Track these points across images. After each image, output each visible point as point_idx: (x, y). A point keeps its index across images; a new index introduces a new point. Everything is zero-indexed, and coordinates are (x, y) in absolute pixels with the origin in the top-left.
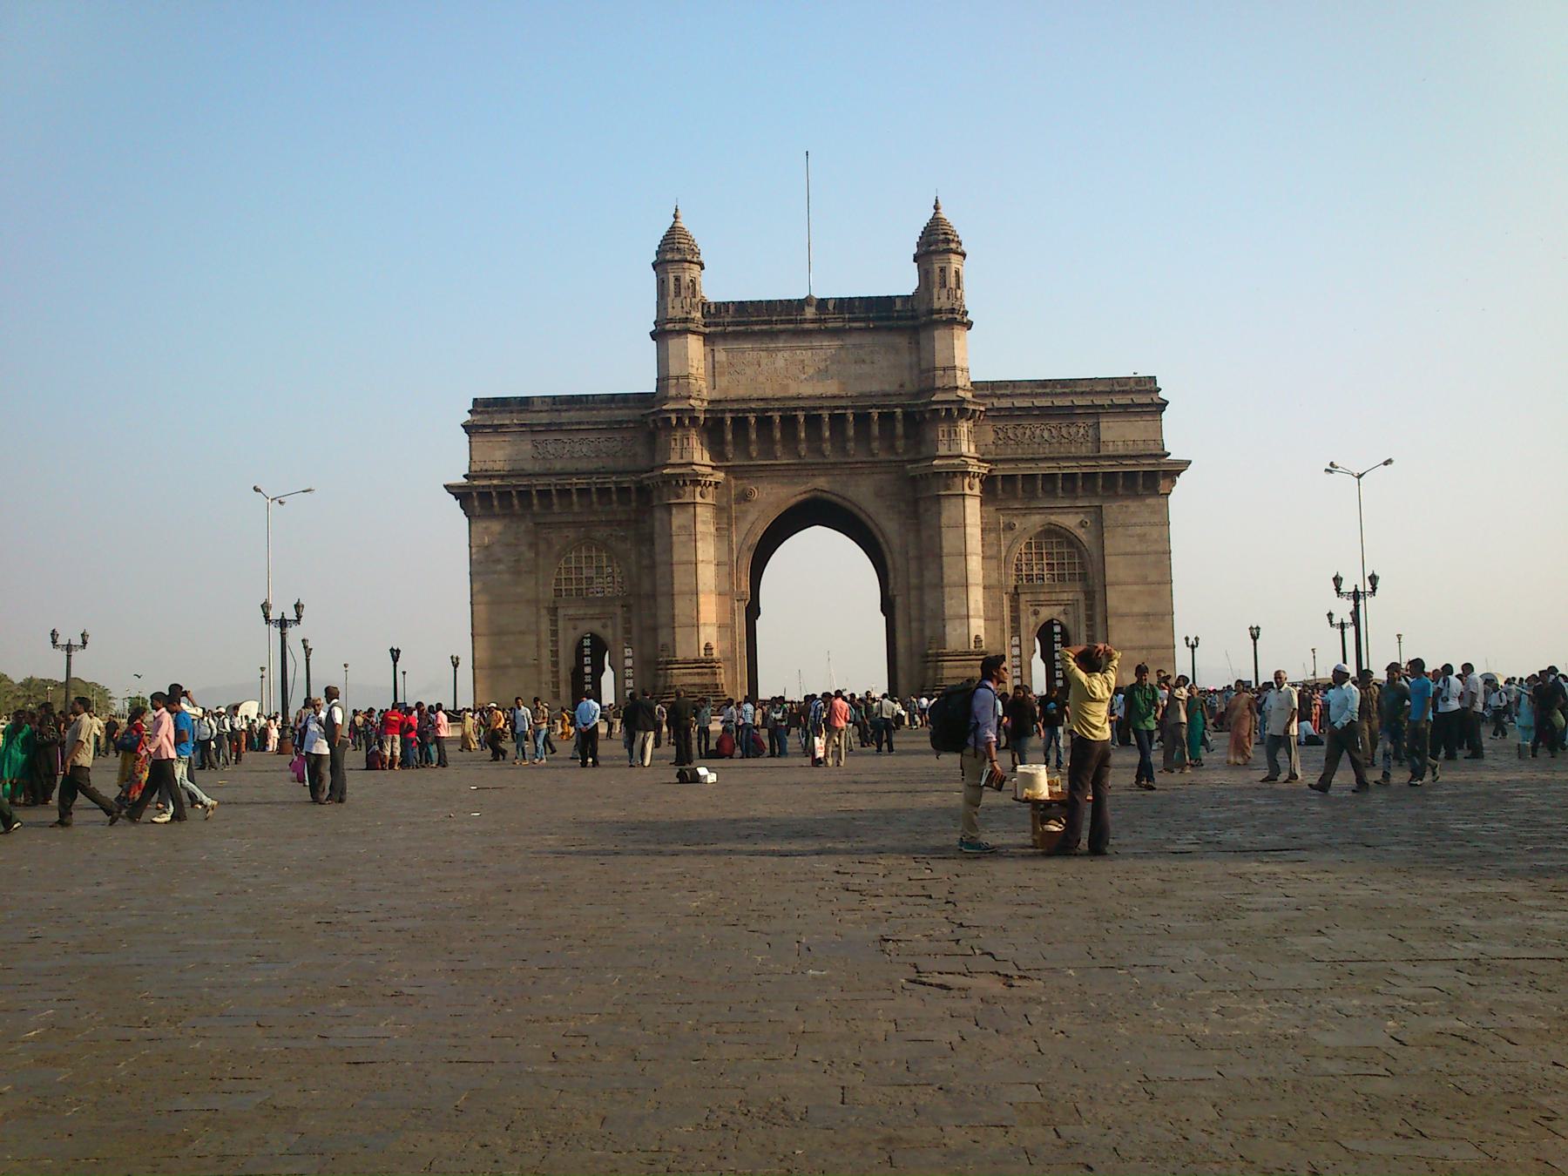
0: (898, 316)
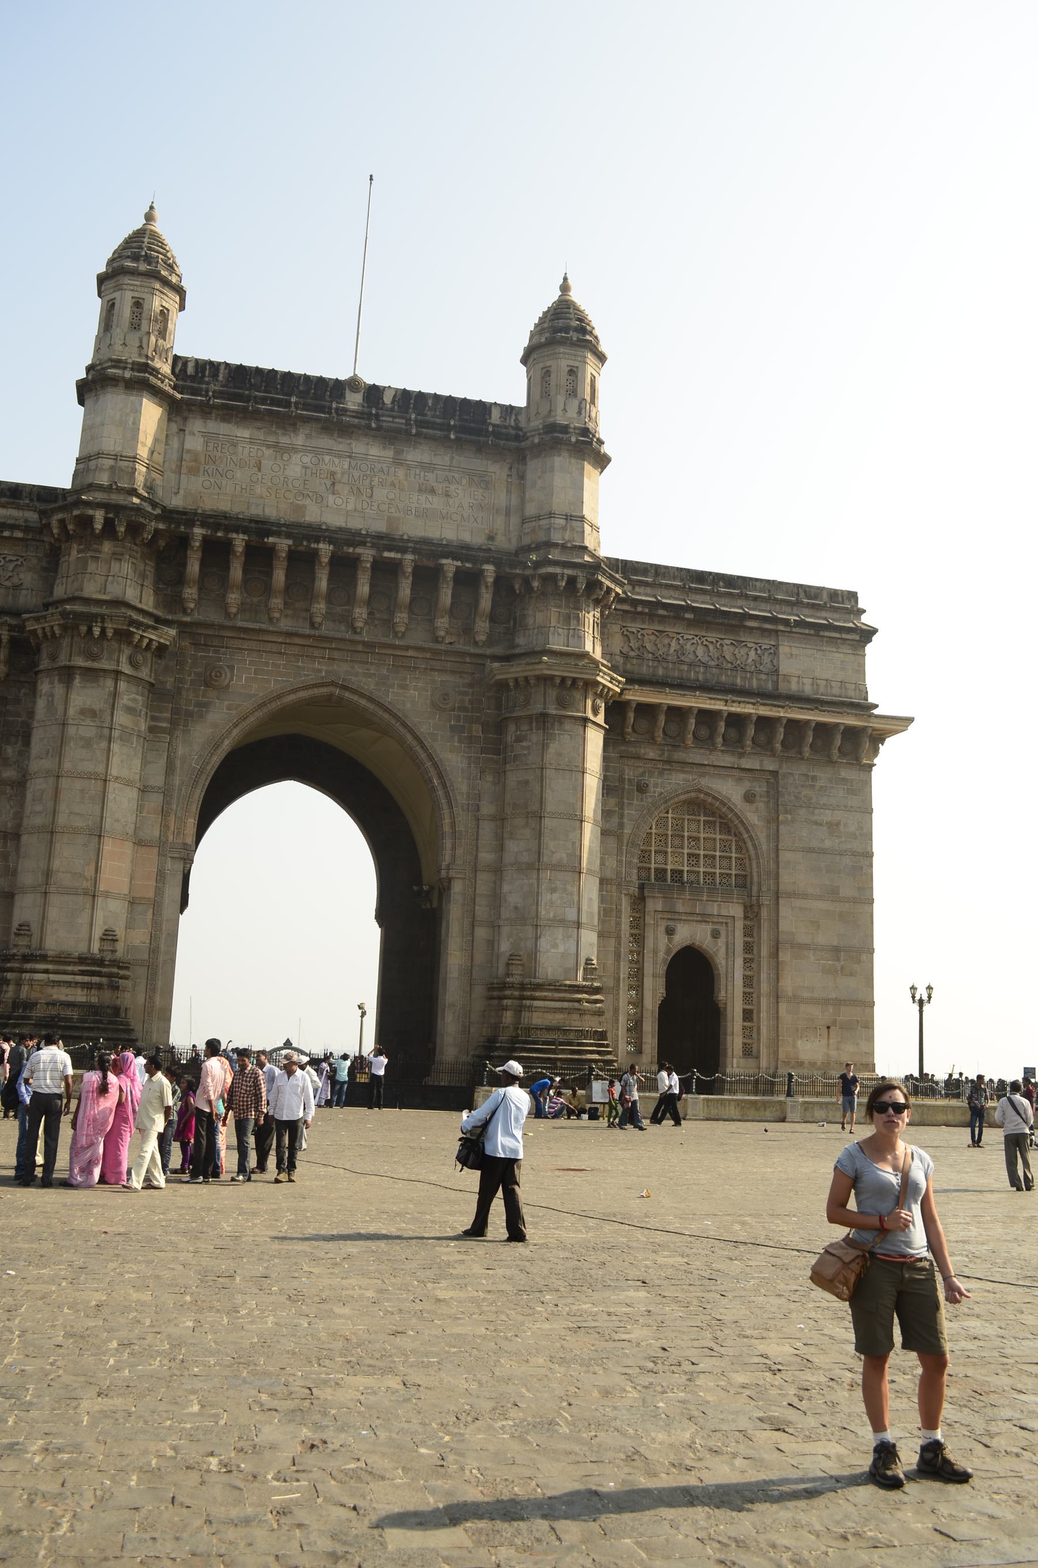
0: (494, 431)
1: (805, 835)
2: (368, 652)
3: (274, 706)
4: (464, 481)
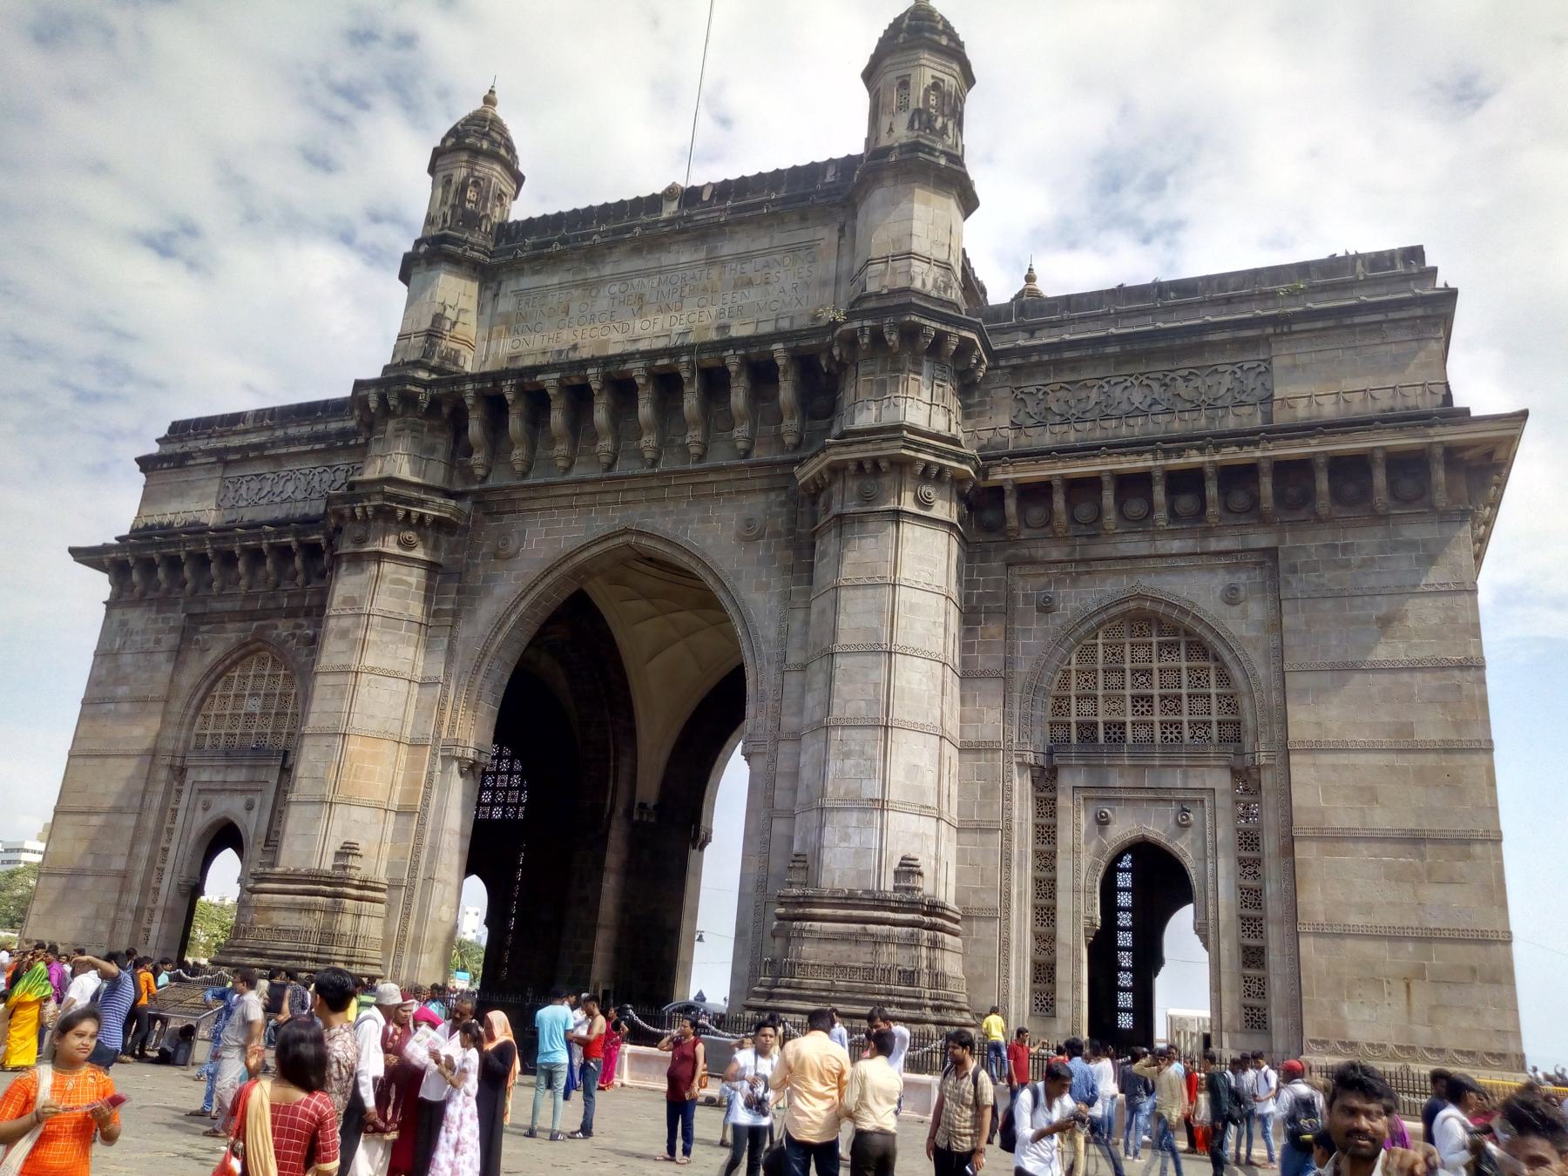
1: (1334, 642)
2: (665, 487)
3: (565, 568)
4: (787, 260)
